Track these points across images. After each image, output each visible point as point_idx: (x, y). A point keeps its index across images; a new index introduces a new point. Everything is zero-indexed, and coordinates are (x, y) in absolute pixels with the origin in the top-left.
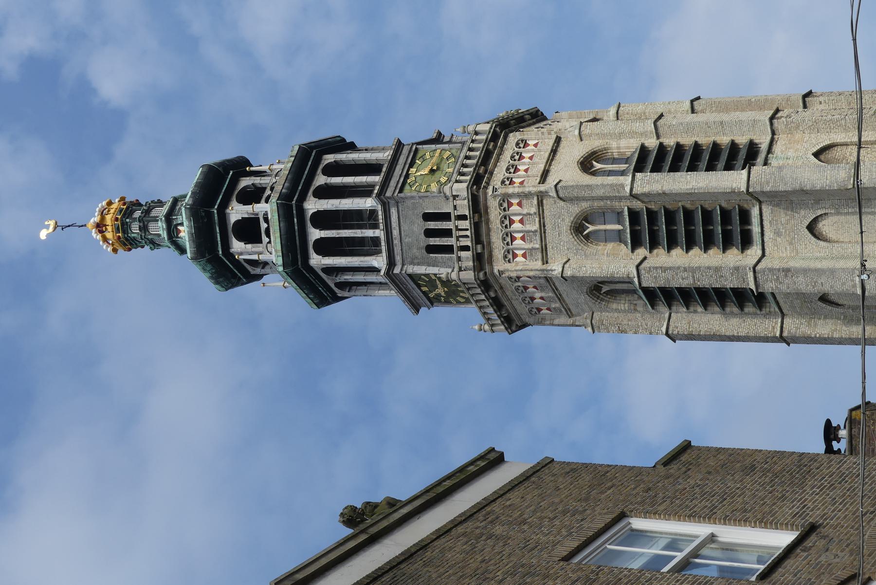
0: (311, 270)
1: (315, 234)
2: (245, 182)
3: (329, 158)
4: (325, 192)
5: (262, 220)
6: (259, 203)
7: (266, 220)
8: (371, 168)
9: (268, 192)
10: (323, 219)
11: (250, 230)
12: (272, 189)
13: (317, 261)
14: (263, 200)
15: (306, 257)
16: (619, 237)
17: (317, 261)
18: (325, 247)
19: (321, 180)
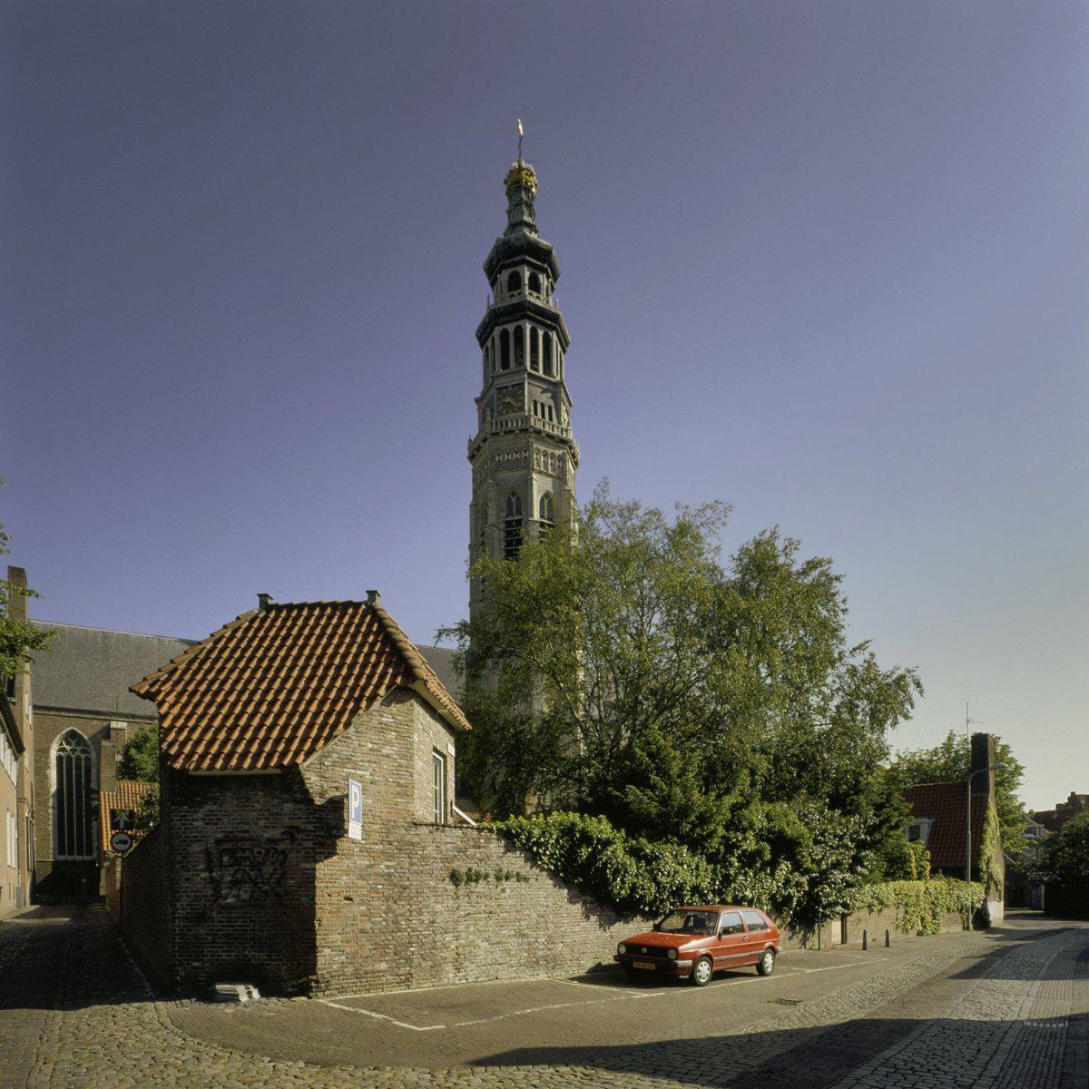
1: (511, 328)
2: (542, 278)
6: (530, 288)
9: (535, 294)
10: (519, 332)
11: (515, 282)
12: (538, 298)
13: (497, 331)
16: (510, 513)
17: (497, 331)
18: (505, 334)
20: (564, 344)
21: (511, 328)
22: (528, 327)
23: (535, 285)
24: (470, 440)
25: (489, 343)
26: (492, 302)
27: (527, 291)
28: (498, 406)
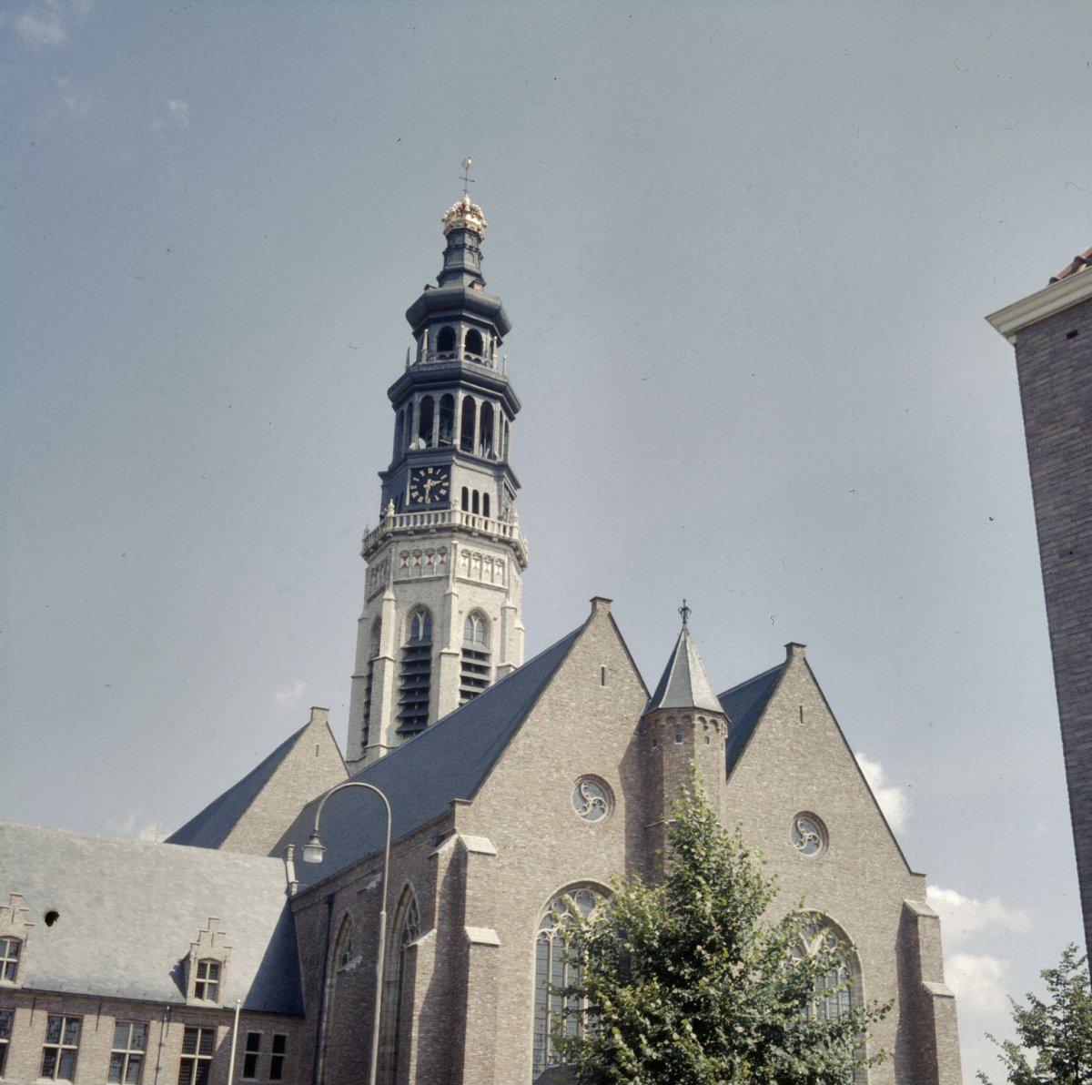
0: (411, 394)
1: (437, 396)
2: (486, 338)
3: (497, 407)
4: (469, 404)
5: (451, 352)
7: (452, 356)
8: (487, 437)
9: (474, 356)
10: (449, 402)
12: (477, 361)
13: (418, 398)
14: (467, 353)
15: (421, 390)
17: (418, 398)
19: (479, 402)
20: (511, 408)
21: (437, 396)
22: (461, 396)
23: (474, 344)
24: (367, 531)
25: (405, 408)
26: (413, 360)
27: (462, 353)
28: (412, 491)
